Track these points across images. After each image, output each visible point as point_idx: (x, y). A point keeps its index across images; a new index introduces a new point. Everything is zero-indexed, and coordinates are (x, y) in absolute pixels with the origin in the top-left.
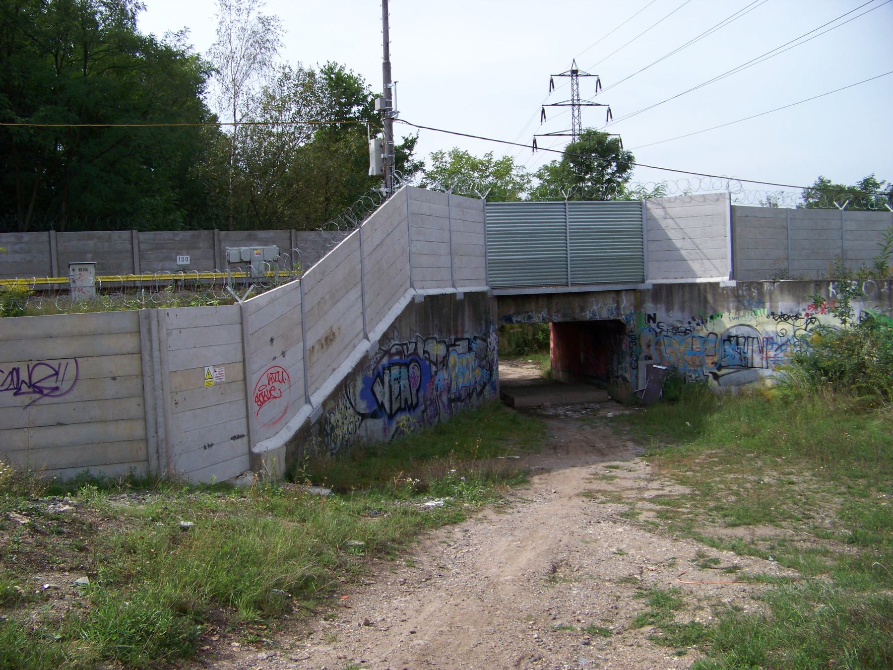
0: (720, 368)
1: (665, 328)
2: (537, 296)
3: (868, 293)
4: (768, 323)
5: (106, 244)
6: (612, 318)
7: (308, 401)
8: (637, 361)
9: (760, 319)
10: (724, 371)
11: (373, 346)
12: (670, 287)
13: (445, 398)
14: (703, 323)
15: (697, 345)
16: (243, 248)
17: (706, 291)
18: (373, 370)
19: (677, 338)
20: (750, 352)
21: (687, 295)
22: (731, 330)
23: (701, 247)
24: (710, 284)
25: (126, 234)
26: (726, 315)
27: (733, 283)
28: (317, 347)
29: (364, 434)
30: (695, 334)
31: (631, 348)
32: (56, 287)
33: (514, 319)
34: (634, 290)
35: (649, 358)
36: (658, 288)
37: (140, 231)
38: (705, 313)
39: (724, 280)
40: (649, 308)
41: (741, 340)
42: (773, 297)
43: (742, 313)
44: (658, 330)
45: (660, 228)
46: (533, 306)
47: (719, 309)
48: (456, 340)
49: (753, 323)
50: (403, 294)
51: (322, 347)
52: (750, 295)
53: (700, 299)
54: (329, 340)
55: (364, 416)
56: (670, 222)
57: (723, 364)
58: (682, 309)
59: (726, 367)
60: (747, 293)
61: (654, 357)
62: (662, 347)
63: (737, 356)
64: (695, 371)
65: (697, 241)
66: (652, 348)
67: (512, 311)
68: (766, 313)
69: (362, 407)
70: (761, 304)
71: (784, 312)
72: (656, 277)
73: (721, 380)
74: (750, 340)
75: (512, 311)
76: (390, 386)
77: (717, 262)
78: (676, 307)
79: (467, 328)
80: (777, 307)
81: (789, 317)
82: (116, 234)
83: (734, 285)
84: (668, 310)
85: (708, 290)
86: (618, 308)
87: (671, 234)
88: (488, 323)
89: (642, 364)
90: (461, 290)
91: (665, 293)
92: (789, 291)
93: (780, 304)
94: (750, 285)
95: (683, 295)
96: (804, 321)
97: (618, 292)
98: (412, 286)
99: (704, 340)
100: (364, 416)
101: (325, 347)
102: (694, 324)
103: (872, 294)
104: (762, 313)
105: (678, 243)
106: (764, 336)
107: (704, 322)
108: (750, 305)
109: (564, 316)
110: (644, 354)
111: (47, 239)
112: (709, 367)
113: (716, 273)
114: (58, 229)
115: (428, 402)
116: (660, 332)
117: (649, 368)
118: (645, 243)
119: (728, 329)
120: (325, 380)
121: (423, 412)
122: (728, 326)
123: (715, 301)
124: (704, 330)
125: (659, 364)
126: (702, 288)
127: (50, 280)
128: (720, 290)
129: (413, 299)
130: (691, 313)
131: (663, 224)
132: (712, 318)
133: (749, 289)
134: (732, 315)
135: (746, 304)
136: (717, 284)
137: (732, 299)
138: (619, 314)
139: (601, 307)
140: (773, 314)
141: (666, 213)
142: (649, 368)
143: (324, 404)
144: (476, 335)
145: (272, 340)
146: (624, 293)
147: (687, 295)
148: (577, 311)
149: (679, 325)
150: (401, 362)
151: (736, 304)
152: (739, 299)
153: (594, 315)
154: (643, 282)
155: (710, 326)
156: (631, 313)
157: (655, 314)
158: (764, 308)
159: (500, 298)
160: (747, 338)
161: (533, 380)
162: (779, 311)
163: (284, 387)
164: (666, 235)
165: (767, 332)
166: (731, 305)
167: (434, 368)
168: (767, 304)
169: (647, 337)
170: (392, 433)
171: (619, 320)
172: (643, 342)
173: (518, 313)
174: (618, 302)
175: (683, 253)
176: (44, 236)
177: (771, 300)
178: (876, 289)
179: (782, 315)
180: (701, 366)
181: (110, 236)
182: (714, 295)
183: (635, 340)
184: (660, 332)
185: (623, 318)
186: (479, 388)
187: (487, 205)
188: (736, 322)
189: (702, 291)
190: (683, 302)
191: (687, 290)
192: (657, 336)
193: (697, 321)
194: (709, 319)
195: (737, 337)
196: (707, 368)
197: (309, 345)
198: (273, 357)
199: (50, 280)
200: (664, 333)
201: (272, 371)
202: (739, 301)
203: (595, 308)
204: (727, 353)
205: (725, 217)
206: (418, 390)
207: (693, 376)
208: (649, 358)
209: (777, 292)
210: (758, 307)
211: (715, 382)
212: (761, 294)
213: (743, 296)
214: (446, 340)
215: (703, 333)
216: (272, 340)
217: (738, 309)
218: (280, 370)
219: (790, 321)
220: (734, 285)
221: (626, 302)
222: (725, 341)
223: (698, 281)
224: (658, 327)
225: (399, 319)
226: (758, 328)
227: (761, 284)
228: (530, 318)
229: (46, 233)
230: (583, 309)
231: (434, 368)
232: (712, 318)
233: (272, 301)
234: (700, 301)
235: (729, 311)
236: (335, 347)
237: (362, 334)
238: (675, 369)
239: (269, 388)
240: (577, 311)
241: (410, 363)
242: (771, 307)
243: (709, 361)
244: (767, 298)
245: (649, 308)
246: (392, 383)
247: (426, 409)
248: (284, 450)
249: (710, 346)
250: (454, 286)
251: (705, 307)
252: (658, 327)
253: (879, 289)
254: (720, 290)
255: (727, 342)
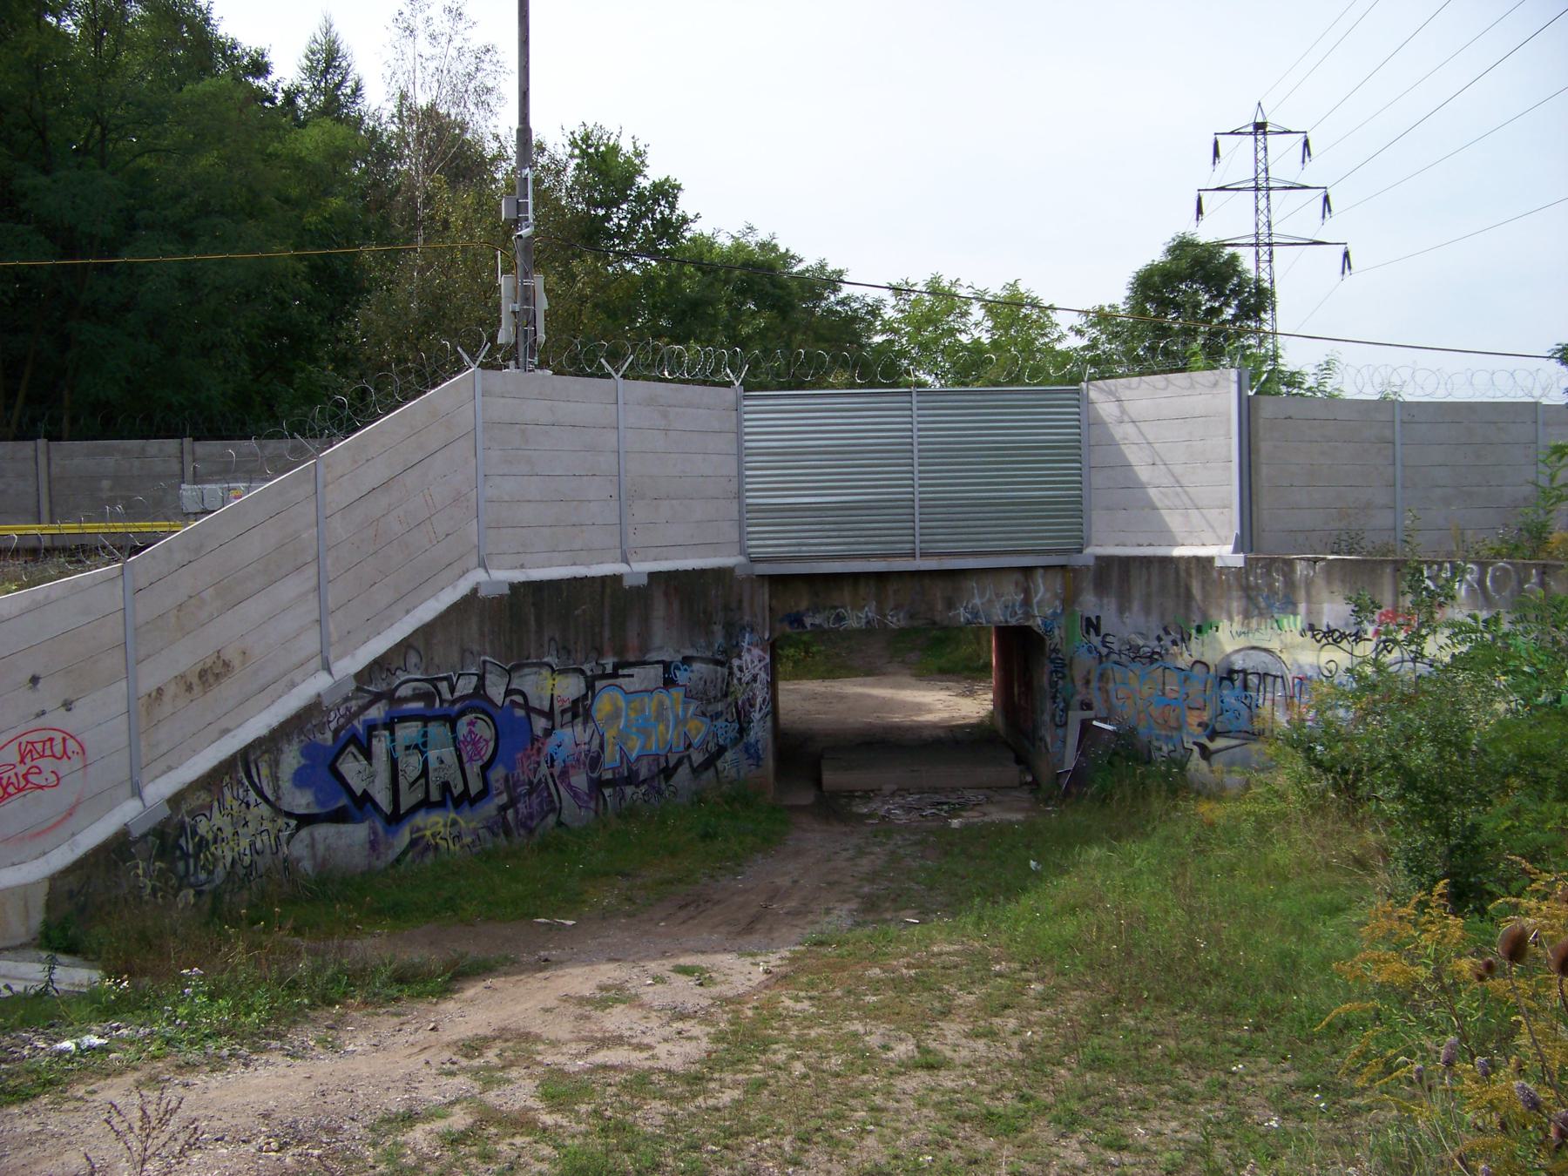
0: (1213, 735)
1: (1115, 647)
2: (856, 577)
3: (1497, 591)
4: (1303, 648)
5: (137, 463)
6: (1013, 622)
7: (137, 792)
8: (1066, 710)
9: (1288, 638)
10: (1220, 743)
11: (337, 685)
12: (1126, 562)
13: (580, 780)
14: (1183, 640)
15: (1173, 686)
16: (208, 486)
17: (1189, 574)
18: (336, 732)
19: (1136, 667)
20: (1268, 704)
21: (1155, 580)
22: (1234, 658)
23: (1184, 482)
24: (1197, 559)
25: (171, 445)
26: (1224, 625)
27: (1238, 561)
28: (171, 690)
29: (305, 853)
30: (1169, 661)
31: (1053, 685)
32: (46, 542)
33: (808, 621)
34: (1063, 567)
35: (1087, 706)
36: (1105, 562)
37: (197, 439)
38: (1188, 619)
39: (1224, 553)
40: (1089, 603)
41: (1253, 680)
42: (1314, 592)
43: (1254, 623)
44: (1104, 651)
45: (1112, 443)
46: (847, 595)
47: (1213, 612)
48: (616, 667)
49: (1274, 645)
50: (453, 582)
51: (189, 688)
52: (1271, 586)
53: (1177, 587)
54: (212, 674)
55: (305, 820)
56: (1129, 429)
57: (1218, 727)
58: (1147, 610)
59: (1225, 734)
60: (1264, 582)
61: (1096, 704)
62: (1111, 686)
63: (1245, 712)
64: (1168, 739)
65: (1178, 470)
66: (1094, 684)
67: (804, 605)
68: (1299, 626)
69: (301, 801)
70: (1290, 606)
71: (1333, 627)
72: (1106, 544)
73: (1215, 758)
74: (1269, 680)
75: (804, 605)
76: (394, 763)
77: (1213, 514)
78: (1136, 606)
79: (657, 640)
80: (1320, 613)
81: (1343, 636)
82: (153, 445)
83: (1240, 564)
84: (1122, 609)
85: (1193, 572)
86: (1027, 602)
87: (1134, 455)
88: (733, 631)
89: (1075, 717)
90: (638, 569)
91: (1117, 574)
92: (1343, 581)
93: (1326, 607)
94: (1270, 564)
95: (1148, 582)
96: (1370, 646)
97: (1027, 571)
98: (483, 565)
99: (1185, 675)
100: (305, 820)
101: (197, 689)
102: (1167, 641)
103: (1506, 593)
104: (1293, 624)
105: (1144, 473)
106: (1295, 673)
107: (1185, 638)
108: (1270, 606)
109: (912, 617)
110: (1078, 698)
111: (32, 453)
112: (1192, 734)
113: (1212, 541)
114: (51, 437)
115: (523, 789)
116: (1108, 655)
117: (1086, 726)
118: (1085, 471)
119: (1228, 656)
120: (195, 752)
121: (503, 809)
122: (1229, 649)
123: (1206, 595)
124: (1186, 655)
125: (1104, 720)
126: (1182, 567)
127: (34, 529)
128: (1215, 574)
129: (475, 591)
130: (1162, 616)
131: (1119, 432)
132: (1199, 630)
133: (1269, 573)
134: (1237, 627)
135: (1263, 605)
136: (1210, 560)
137: (1236, 593)
138: (1028, 615)
139: (990, 601)
140: (1312, 628)
141: (1123, 412)
142: (1086, 726)
143: (175, 800)
144: (689, 652)
145: (35, 680)
146: (1041, 571)
147: (1155, 580)
148: (940, 606)
149: (1141, 643)
150: (429, 713)
151: (1243, 602)
152: (1249, 593)
153: (976, 615)
154: (1080, 551)
155: (1197, 649)
156: (1054, 614)
157: (1098, 618)
158: (1295, 614)
159: (779, 582)
160: (1263, 676)
161: (972, 726)
162: (1325, 622)
163: (64, 767)
164: (1122, 455)
165: (1300, 667)
166: (1236, 605)
167: (540, 724)
168: (1302, 607)
169: (1084, 662)
170: (398, 850)
171: (1029, 628)
172: (1078, 673)
173: (816, 609)
174: (1027, 591)
175: (1152, 492)
176: (26, 448)
177: (1309, 599)
178: (1513, 583)
179: (1330, 632)
180: (1179, 728)
181: (143, 449)
182: (1204, 582)
183: (1063, 667)
184: (1108, 655)
185: (1037, 623)
186: (698, 758)
187: (746, 398)
188: (1242, 642)
189: (1183, 574)
190: (1149, 595)
191: (1155, 570)
192: (1101, 662)
193: (1174, 635)
194: (1193, 632)
195: (1244, 672)
196: (1189, 734)
197: (148, 684)
198: (37, 709)
199: (34, 529)
200: (1114, 657)
201: (24, 739)
202: (1249, 598)
203: (977, 601)
204: (1226, 707)
205: (1229, 420)
206: (485, 768)
207: (1165, 748)
208: (1087, 706)
209: (1320, 582)
210: (1283, 610)
211: (1203, 764)
212: (1290, 584)
213: (1257, 586)
214: (586, 667)
215: (1184, 660)
216: (35, 680)
217: (1247, 616)
218: (58, 737)
219: (1344, 644)
220: (1240, 564)
221: (1043, 590)
222: (1222, 679)
223: (1177, 552)
224: (1104, 643)
225: (426, 631)
226: (1284, 657)
227: (1290, 564)
228: (840, 618)
229: (31, 443)
230: (950, 604)
231: (540, 724)
232: (1199, 630)
233: (37, 607)
234: (1178, 596)
235: (1231, 619)
236: (227, 690)
237: (317, 662)
238: (1133, 731)
239: (22, 769)
240: (940, 606)
241: (462, 713)
242: (1309, 612)
243: (1193, 719)
244: (1302, 593)
245: (1089, 603)
246: (400, 753)
247: (513, 802)
248: (45, 887)
249: (1195, 688)
250: (626, 561)
251: (1188, 607)
252: (1104, 643)
253: (1521, 583)
254: (1215, 574)
255: (1226, 683)
